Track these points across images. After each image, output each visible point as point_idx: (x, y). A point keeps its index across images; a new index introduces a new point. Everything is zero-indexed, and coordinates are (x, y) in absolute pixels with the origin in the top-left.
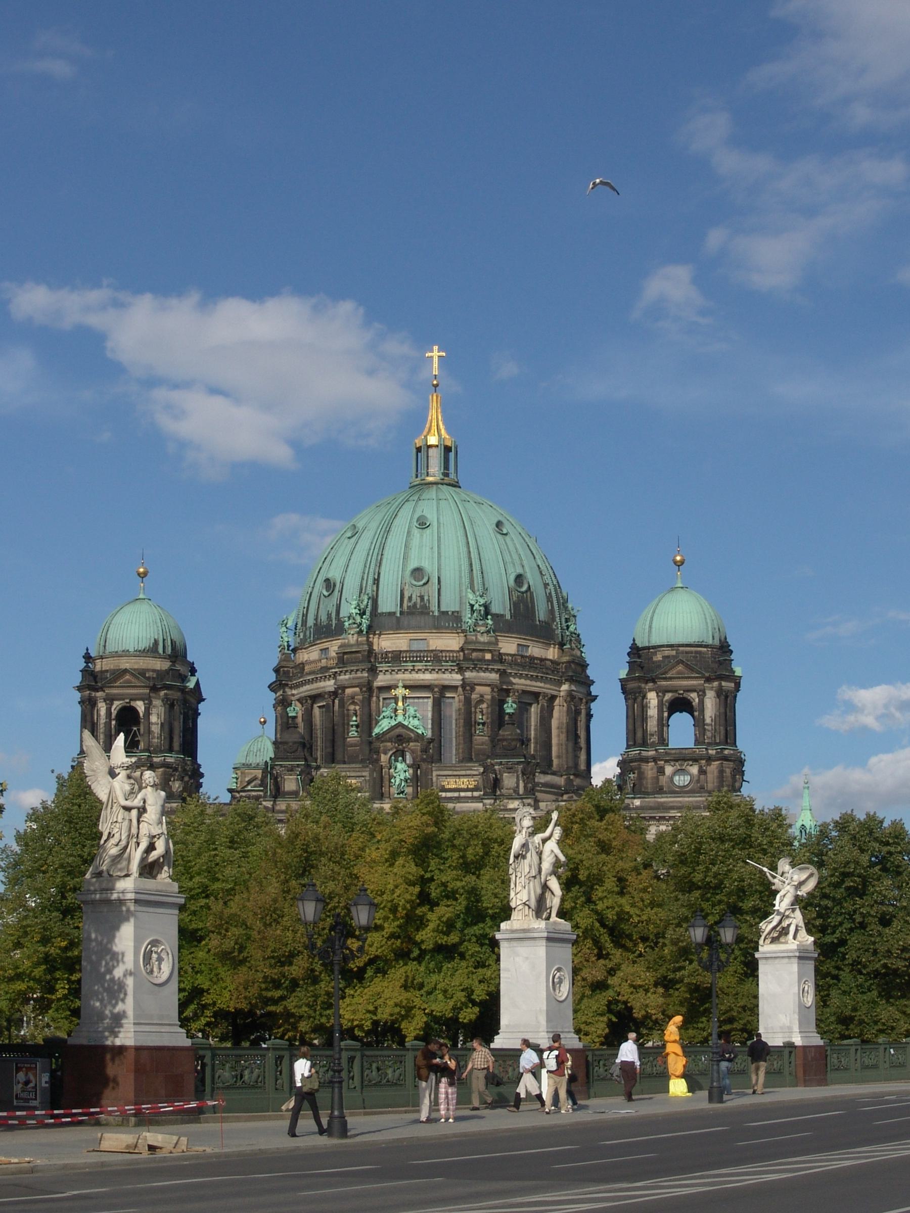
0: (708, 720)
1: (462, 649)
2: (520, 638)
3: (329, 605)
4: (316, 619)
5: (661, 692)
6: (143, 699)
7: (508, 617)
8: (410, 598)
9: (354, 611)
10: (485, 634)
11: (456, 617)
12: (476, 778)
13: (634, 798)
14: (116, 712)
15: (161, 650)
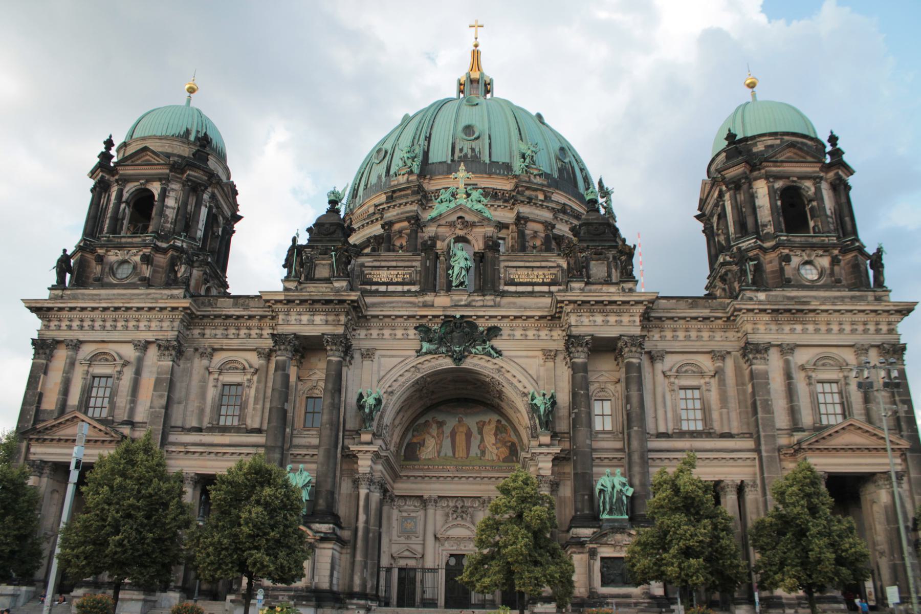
0: (829, 212)
1: (516, 186)
2: (566, 197)
3: (381, 169)
4: (366, 185)
5: (767, 177)
6: (160, 180)
7: (556, 175)
8: (461, 150)
9: (406, 155)
10: (538, 177)
11: (508, 167)
12: (554, 271)
13: (757, 291)
14: (128, 195)
15: (192, 138)
